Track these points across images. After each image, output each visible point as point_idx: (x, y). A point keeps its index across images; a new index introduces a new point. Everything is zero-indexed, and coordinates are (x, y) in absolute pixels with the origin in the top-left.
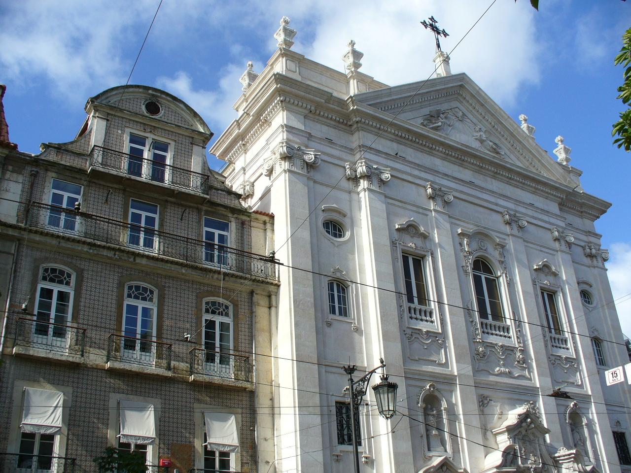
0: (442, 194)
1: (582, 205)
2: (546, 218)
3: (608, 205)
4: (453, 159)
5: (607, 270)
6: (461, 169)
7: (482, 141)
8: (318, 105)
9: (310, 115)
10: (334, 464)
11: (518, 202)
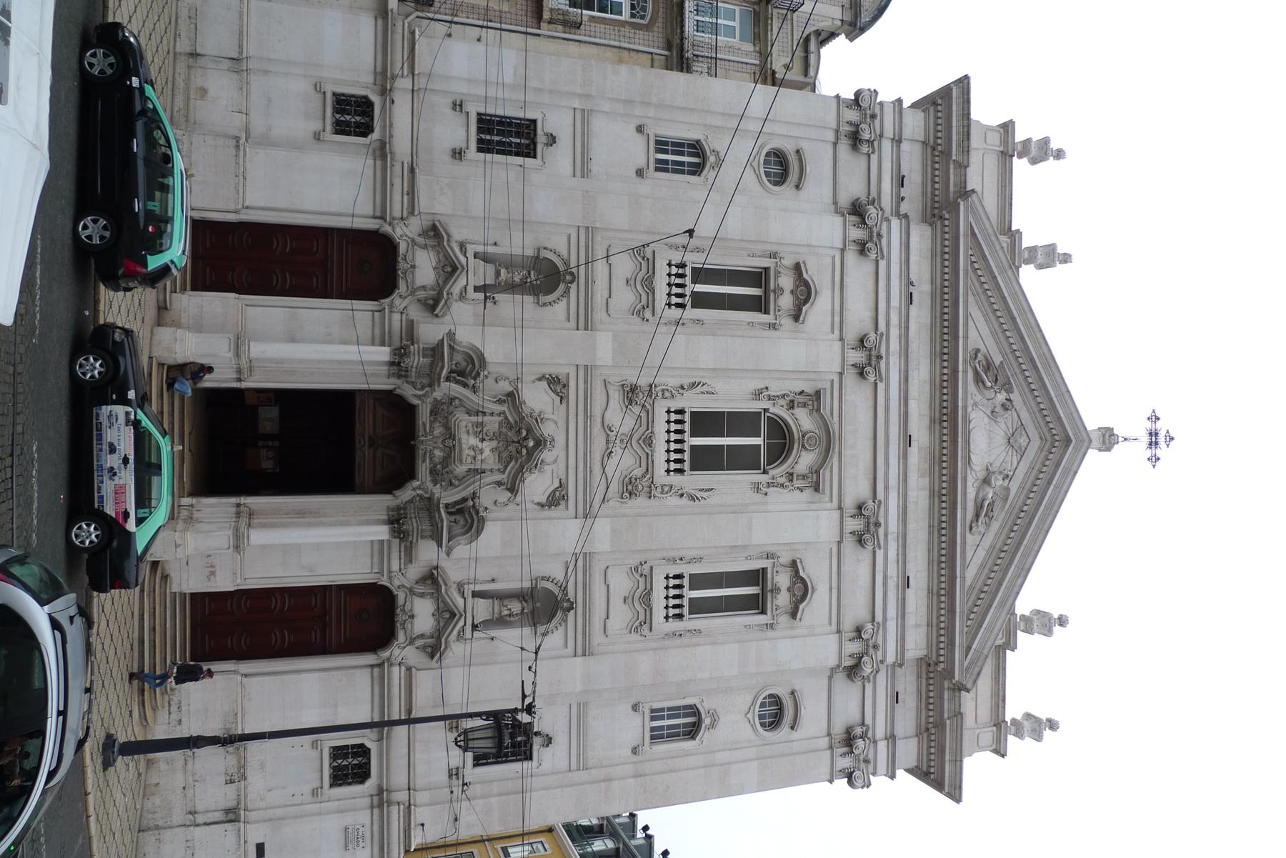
0: (873, 363)
1: (940, 725)
2: (892, 612)
3: (955, 794)
4: (937, 401)
5: (831, 781)
6: (928, 422)
7: (986, 481)
8: (947, 154)
9: (929, 150)
10: (450, 101)
11: (903, 537)
